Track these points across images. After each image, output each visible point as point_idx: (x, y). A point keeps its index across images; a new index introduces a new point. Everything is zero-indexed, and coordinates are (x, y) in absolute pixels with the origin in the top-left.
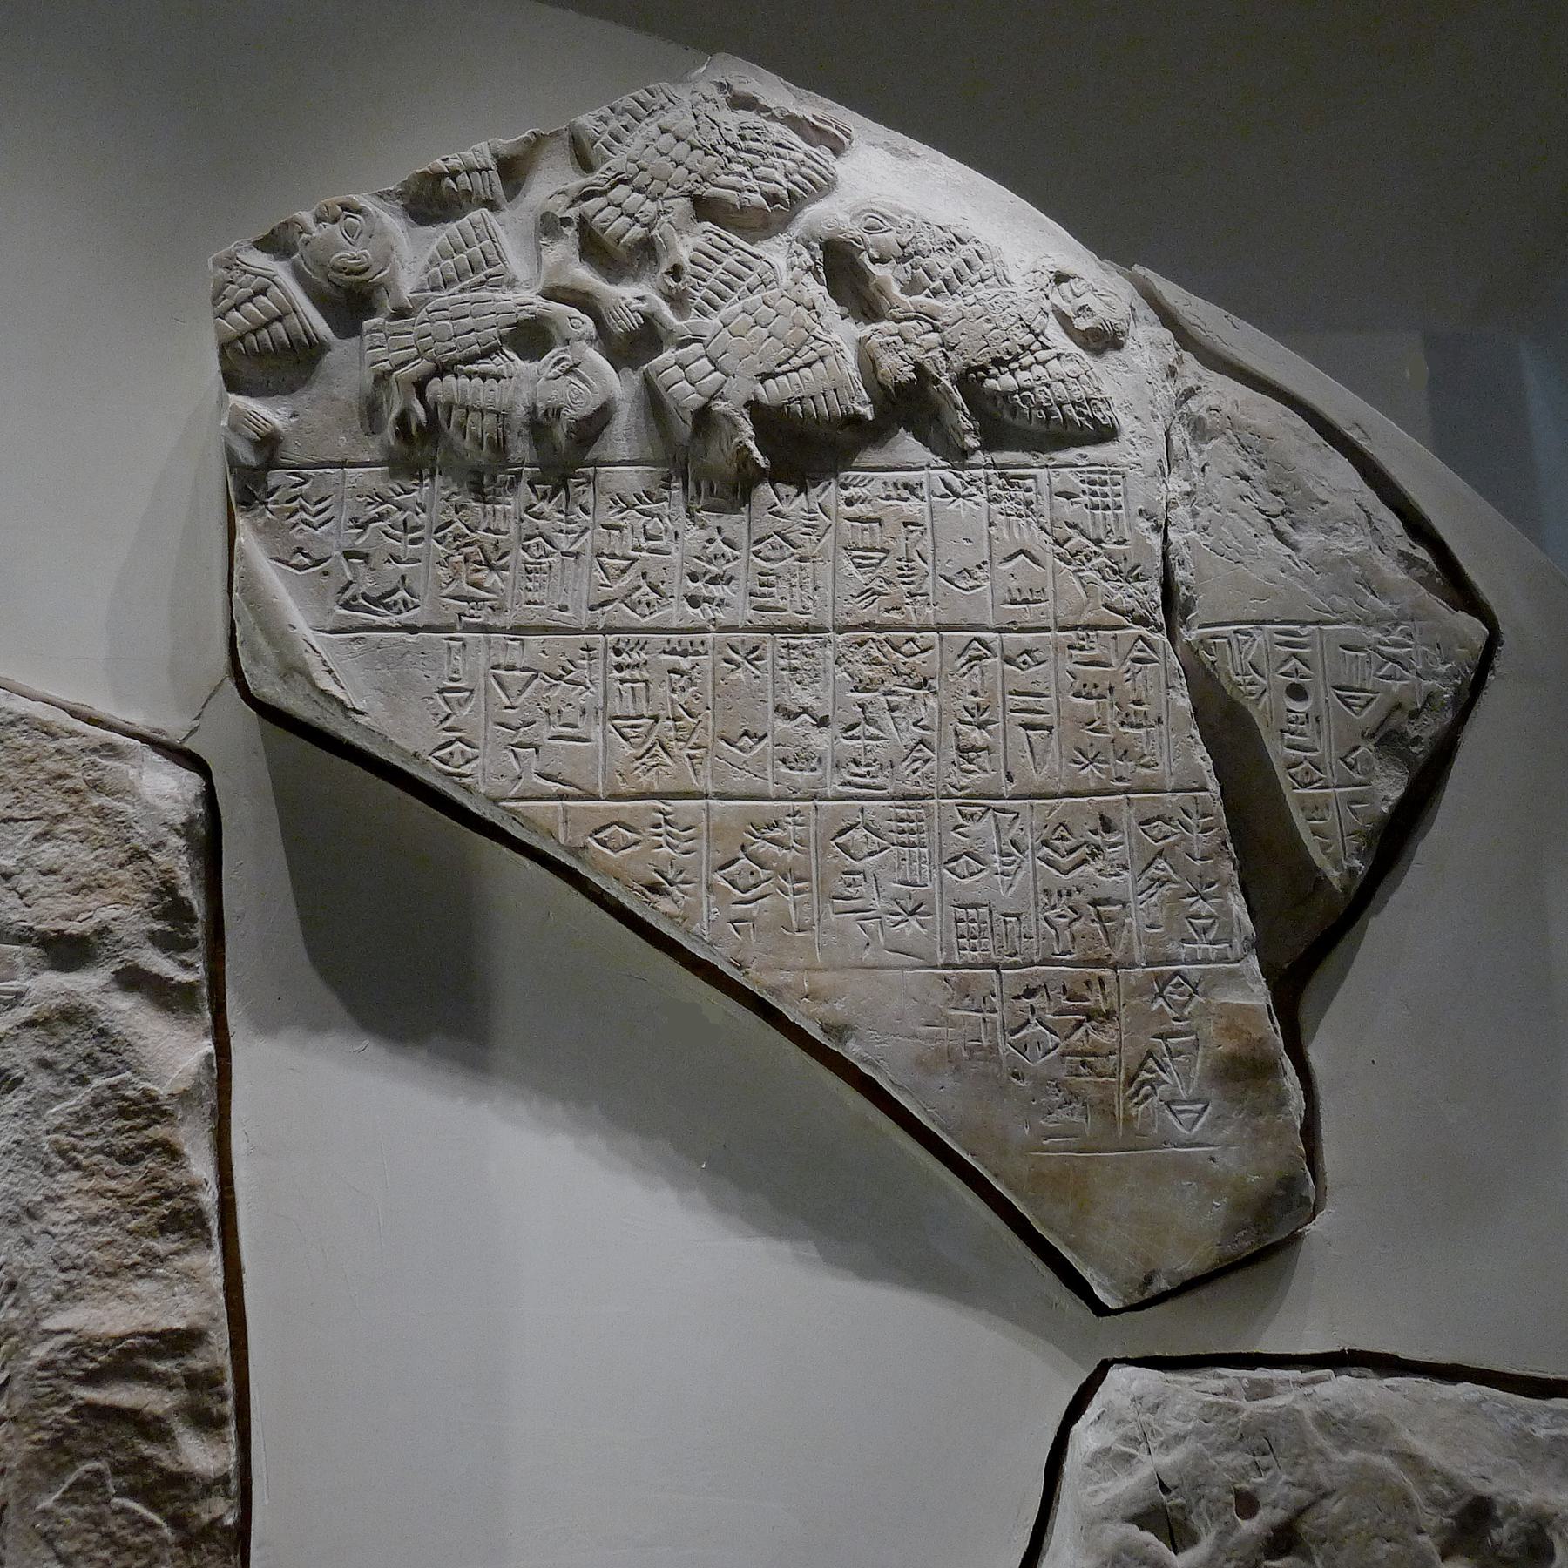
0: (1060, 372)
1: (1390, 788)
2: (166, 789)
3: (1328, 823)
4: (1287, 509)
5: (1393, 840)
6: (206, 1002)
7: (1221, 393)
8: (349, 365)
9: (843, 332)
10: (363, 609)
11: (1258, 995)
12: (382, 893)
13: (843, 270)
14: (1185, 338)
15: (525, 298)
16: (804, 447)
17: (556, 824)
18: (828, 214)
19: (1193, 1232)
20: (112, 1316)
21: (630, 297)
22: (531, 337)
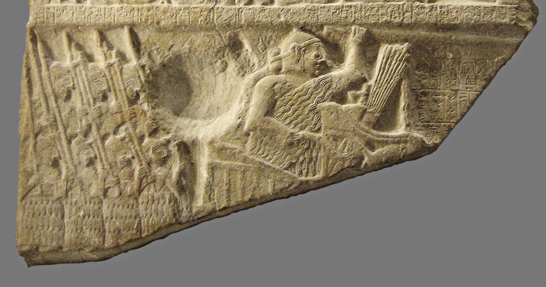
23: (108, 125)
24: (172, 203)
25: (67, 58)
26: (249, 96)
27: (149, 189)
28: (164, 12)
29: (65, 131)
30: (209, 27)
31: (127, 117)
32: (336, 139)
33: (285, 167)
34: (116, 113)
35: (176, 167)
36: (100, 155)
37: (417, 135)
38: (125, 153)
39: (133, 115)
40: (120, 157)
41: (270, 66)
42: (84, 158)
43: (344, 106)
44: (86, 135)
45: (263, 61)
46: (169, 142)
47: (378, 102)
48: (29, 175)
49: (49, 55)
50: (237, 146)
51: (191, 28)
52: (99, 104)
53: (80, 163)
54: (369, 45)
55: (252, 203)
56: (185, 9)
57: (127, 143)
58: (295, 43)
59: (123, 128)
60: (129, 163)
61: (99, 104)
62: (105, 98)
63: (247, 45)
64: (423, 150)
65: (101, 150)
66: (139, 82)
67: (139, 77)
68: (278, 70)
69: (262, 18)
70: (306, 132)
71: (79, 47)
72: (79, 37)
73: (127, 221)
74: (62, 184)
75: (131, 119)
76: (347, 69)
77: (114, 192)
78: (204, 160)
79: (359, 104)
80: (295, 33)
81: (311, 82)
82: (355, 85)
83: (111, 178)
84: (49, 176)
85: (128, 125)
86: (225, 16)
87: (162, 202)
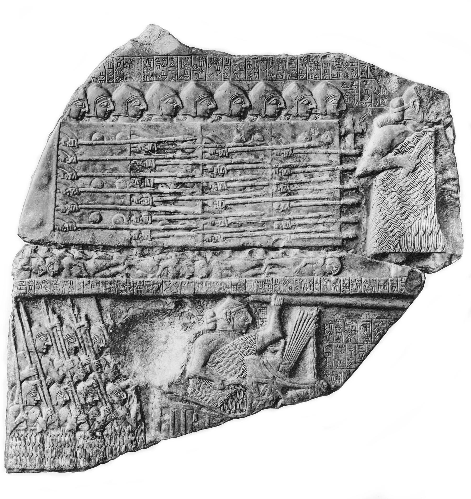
24: (130, 435)
27: (112, 424)
28: (124, 285)
29: (45, 379)
31: (94, 368)
33: (218, 406)
34: (86, 365)
36: (73, 397)
38: (93, 396)
46: (128, 387)
52: (72, 357)
53: (57, 404)
56: (140, 282)
57: (95, 388)
58: (226, 309)
59: (91, 376)
61: (72, 357)
65: (75, 394)
66: (104, 340)
67: (104, 336)
68: (213, 330)
73: (95, 449)
75: (97, 370)
76: (268, 328)
78: (155, 401)
82: (275, 341)
85: (95, 374)
87: (123, 434)
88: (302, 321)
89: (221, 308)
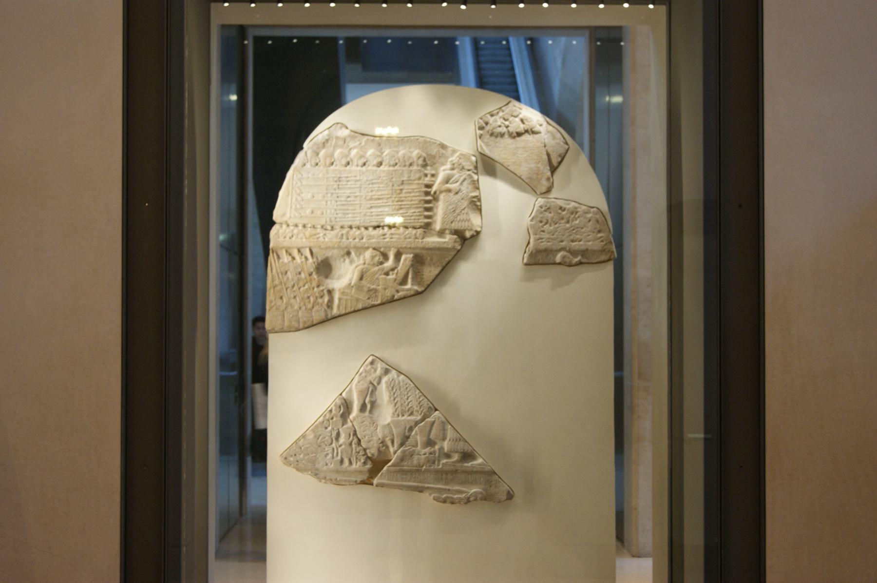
0: (537, 128)
1: (560, 159)
2: (474, 159)
3: (555, 162)
4: (554, 138)
5: (560, 163)
6: (477, 174)
7: (550, 128)
8: (488, 128)
9: (522, 126)
10: (487, 145)
11: (549, 174)
12: (488, 166)
13: (522, 121)
14: (548, 123)
15: (499, 123)
16: (519, 134)
17: (501, 161)
18: (521, 116)
19: (544, 189)
20: (474, 194)
21: (507, 123)
22: (500, 126)
23: (301, 284)
25: (286, 259)
26: (353, 272)
30: (339, 247)
32: (385, 289)
35: (326, 299)
37: (416, 288)
39: (311, 280)
40: (306, 296)
41: (362, 262)
42: (292, 296)
43: (389, 277)
44: (293, 287)
45: (359, 259)
47: (401, 275)
48: (271, 302)
49: (279, 257)
50: (348, 291)
51: (334, 248)
54: (398, 256)
55: (355, 311)
60: (309, 297)
62: (300, 273)
63: (353, 254)
64: (418, 293)
69: (359, 245)
70: (374, 287)
71: (290, 255)
72: (290, 251)
74: (284, 306)
77: (304, 308)
79: (394, 276)
80: (371, 250)
81: (376, 268)
82: (393, 270)
83: (302, 304)
84: (279, 302)
86: (345, 244)
88: (406, 259)
89: (368, 254)
